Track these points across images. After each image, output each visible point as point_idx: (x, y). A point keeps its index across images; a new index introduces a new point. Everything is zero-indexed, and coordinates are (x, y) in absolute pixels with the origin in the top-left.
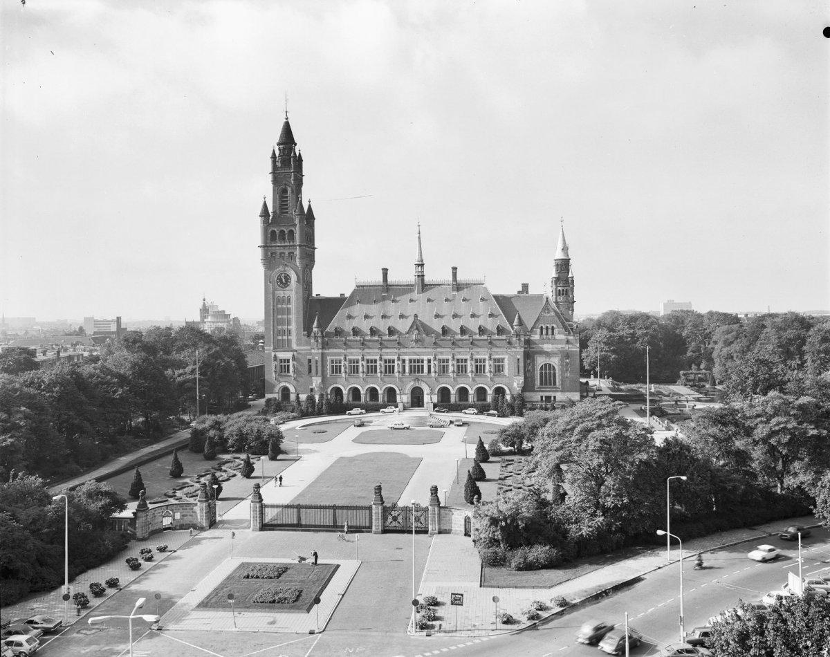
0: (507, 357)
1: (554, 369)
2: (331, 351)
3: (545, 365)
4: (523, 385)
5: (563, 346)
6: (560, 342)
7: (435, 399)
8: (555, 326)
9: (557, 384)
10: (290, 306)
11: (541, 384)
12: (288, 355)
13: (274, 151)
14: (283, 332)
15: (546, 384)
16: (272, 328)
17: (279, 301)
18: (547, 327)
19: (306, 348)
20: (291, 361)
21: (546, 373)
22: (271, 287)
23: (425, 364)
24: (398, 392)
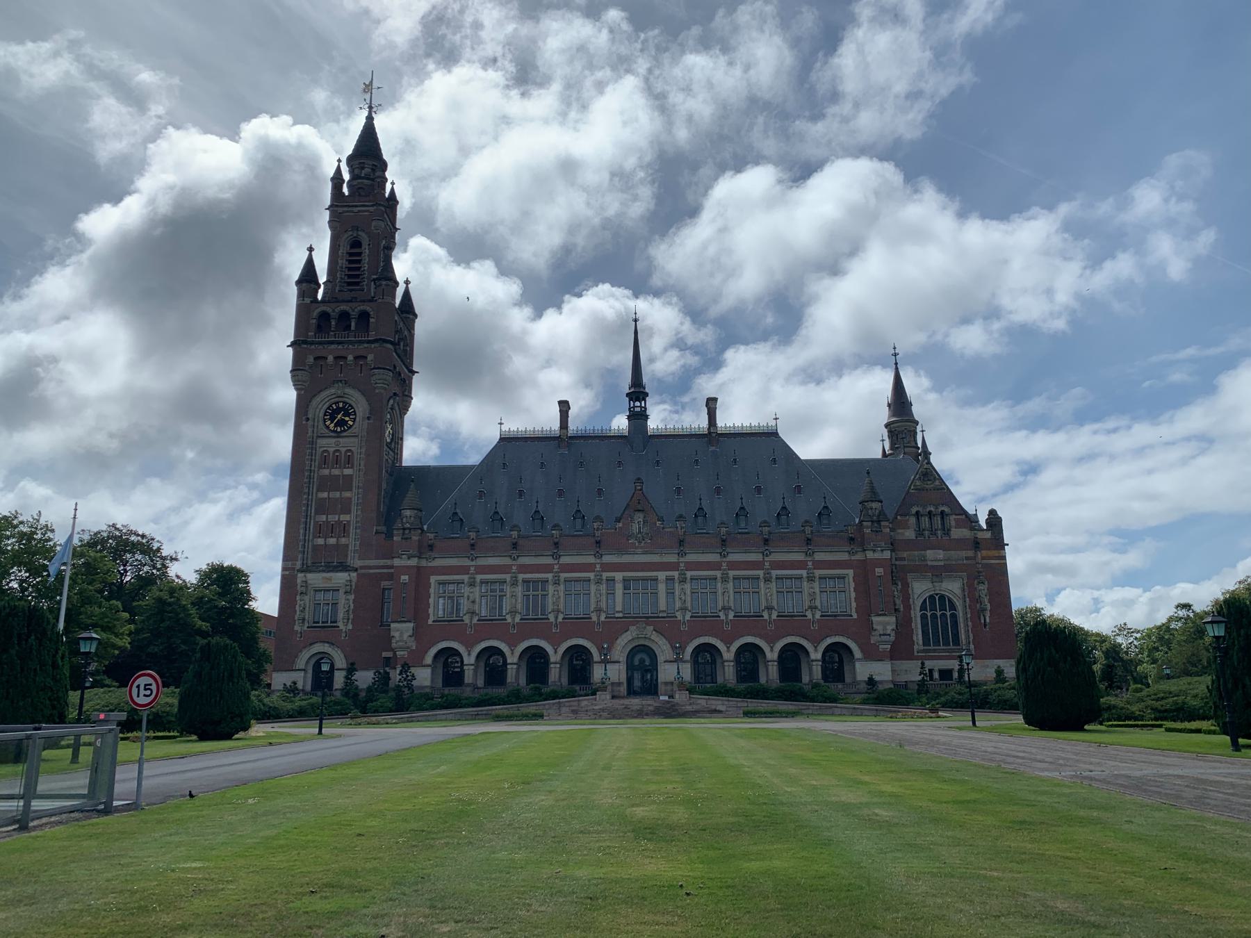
0: (851, 572)
1: (953, 607)
2: (438, 563)
3: (932, 597)
4: (892, 638)
5: (970, 553)
6: (961, 543)
7: (687, 672)
8: (946, 509)
9: (963, 636)
10: (347, 472)
11: (926, 642)
12: (341, 578)
13: (339, 168)
14: (331, 529)
15: (937, 643)
16: (303, 520)
17: (324, 462)
18: (930, 512)
19: (382, 562)
20: (342, 591)
21: (934, 616)
22: (310, 430)
23: (662, 588)
24: (596, 656)
